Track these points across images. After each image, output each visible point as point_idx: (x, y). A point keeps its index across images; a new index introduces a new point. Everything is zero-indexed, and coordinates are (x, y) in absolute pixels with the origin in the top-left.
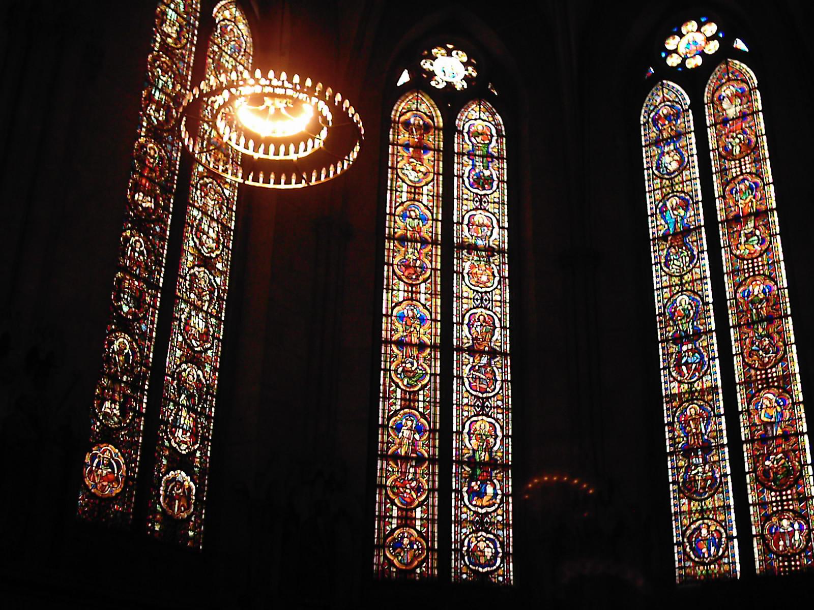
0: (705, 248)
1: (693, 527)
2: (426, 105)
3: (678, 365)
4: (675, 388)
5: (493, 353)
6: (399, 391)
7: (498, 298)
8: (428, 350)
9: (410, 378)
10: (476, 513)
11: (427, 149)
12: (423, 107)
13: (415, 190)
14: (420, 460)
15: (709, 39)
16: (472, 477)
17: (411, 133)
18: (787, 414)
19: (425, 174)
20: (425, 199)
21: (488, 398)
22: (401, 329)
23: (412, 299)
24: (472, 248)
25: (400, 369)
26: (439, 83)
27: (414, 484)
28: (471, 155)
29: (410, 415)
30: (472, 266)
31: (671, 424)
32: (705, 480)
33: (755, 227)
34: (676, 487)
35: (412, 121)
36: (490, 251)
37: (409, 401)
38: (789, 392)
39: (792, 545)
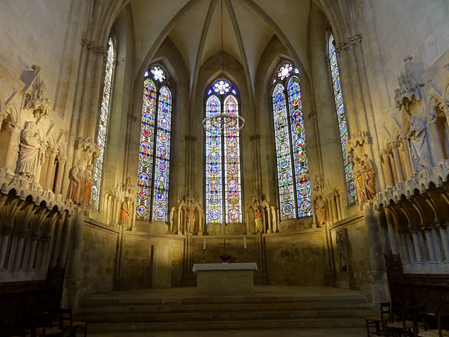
0: (221, 142)
1: (212, 211)
2: (152, 84)
3: (211, 171)
4: (210, 176)
5: (165, 160)
6: (142, 167)
7: (167, 144)
8: (150, 157)
9: (145, 164)
10: (159, 203)
11: (152, 98)
12: (151, 85)
13: (148, 109)
14: (146, 187)
15: (226, 88)
16: (159, 193)
17: (148, 92)
18: (237, 187)
19: (151, 105)
20: (151, 113)
21: (164, 172)
22: (143, 149)
23: (146, 141)
24: (162, 129)
25: (142, 161)
26: (156, 78)
27: (145, 193)
28: (163, 102)
29: (145, 174)
30: (162, 135)
31: (208, 185)
32: (215, 200)
33: (234, 140)
34: (208, 201)
35: (149, 88)
36: (166, 131)
37: (145, 170)
38: (238, 181)
39: (235, 217)
